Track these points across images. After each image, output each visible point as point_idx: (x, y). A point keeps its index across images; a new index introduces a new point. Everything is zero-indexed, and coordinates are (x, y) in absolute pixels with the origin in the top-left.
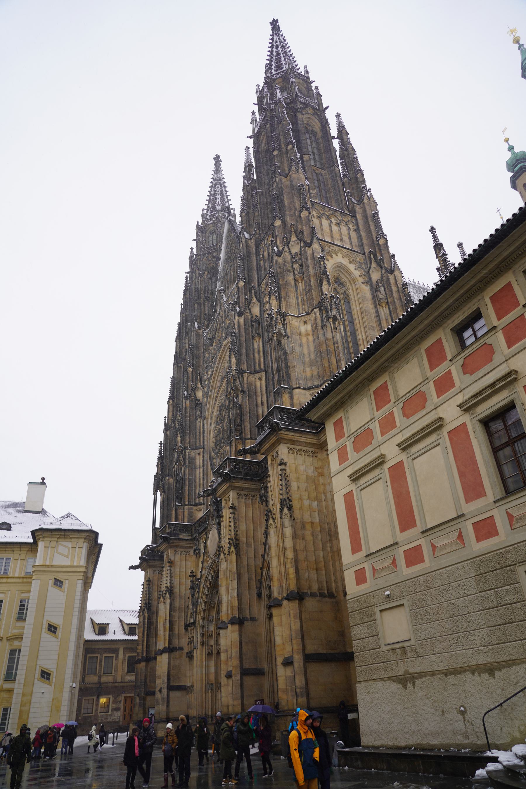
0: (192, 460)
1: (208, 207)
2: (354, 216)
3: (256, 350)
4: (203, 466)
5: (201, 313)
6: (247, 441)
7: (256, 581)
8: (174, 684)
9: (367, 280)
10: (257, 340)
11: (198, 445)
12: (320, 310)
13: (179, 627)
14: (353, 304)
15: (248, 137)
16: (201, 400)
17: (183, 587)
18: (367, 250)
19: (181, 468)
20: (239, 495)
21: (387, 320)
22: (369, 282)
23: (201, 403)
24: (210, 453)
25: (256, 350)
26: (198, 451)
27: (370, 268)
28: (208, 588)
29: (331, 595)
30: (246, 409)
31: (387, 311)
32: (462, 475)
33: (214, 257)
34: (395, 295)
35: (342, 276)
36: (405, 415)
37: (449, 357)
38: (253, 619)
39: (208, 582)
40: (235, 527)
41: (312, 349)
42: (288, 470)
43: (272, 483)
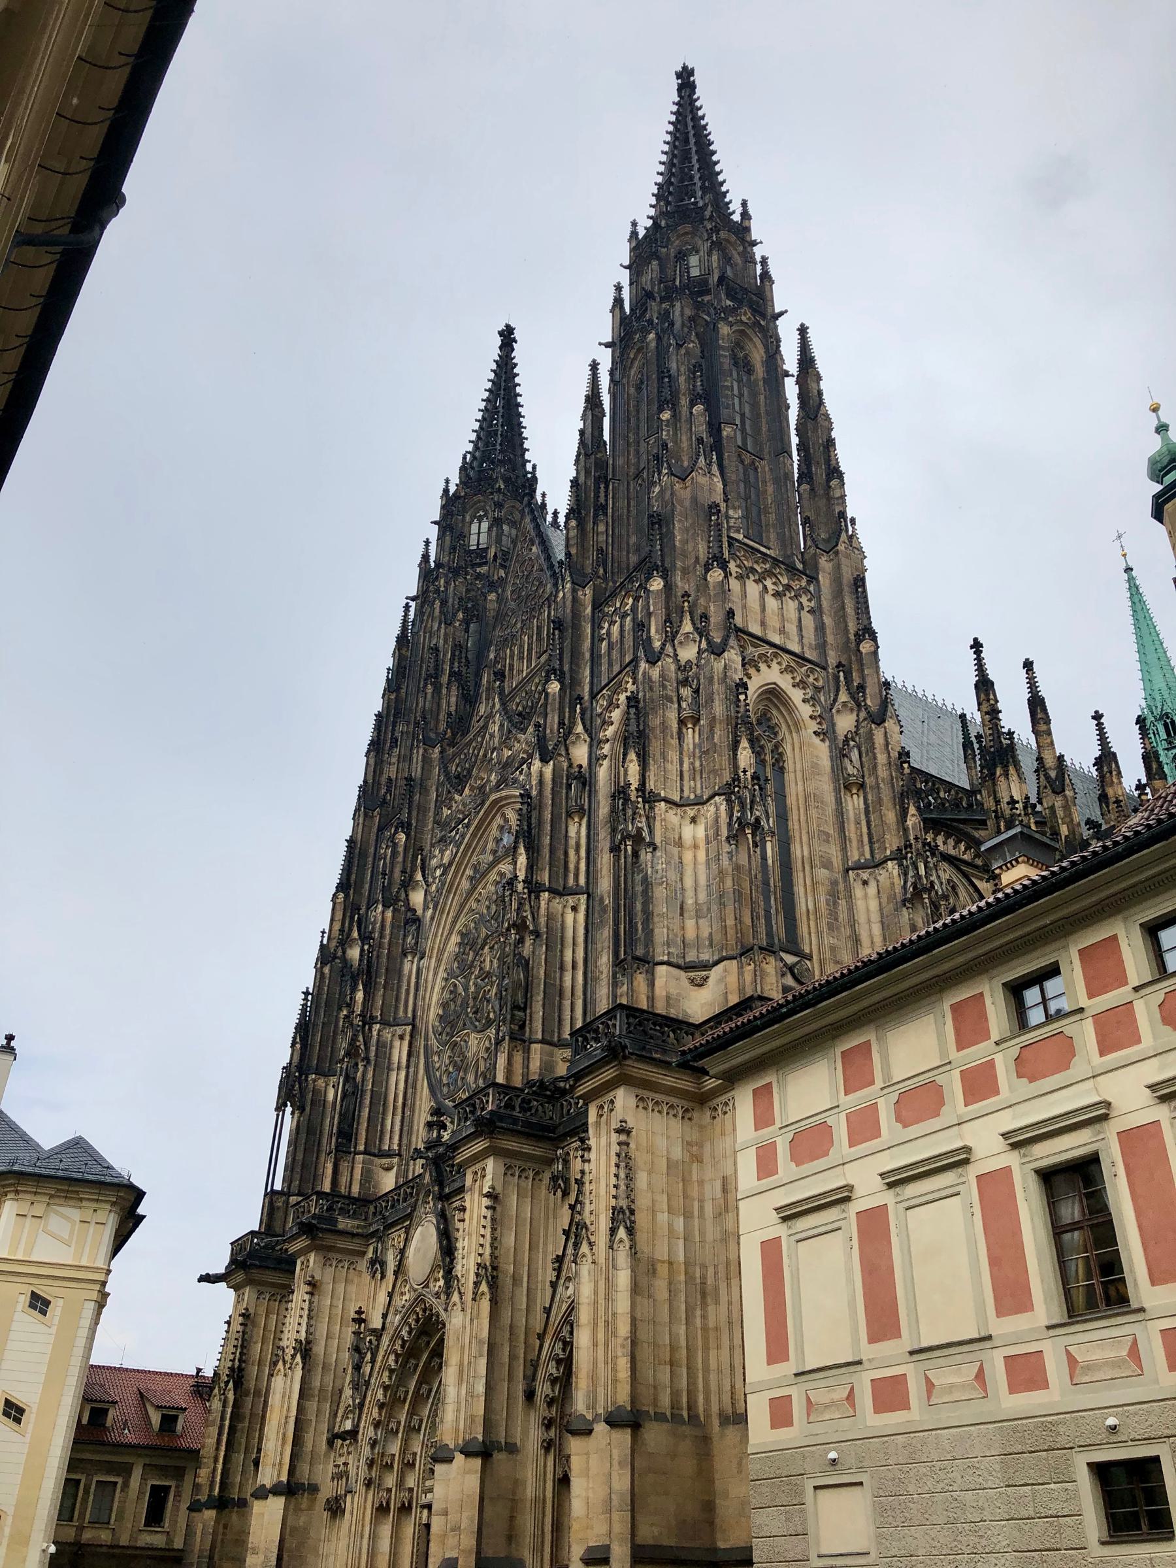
0: (384, 1049)
2: (813, 579)
3: (572, 842)
4: (408, 1067)
5: (439, 705)
6: (533, 1046)
7: (539, 1370)
9: (824, 726)
10: (576, 820)
11: (401, 1014)
12: (729, 802)
13: (316, 1438)
14: (789, 777)
16: (419, 912)
17: (335, 1347)
19: (357, 1064)
20: (509, 1168)
21: (858, 823)
22: (826, 733)
23: (418, 920)
24: (426, 1039)
26: (399, 1030)
27: (835, 701)
28: (397, 1356)
32: (994, 1262)
33: (479, 576)
34: (883, 772)
35: (774, 712)
36: (898, 1120)
37: (995, 1035)
38: (511, 1449)
40: (494, 1239)
41: (703, 880)
42: (632, 1146)
43: (593, 1165)
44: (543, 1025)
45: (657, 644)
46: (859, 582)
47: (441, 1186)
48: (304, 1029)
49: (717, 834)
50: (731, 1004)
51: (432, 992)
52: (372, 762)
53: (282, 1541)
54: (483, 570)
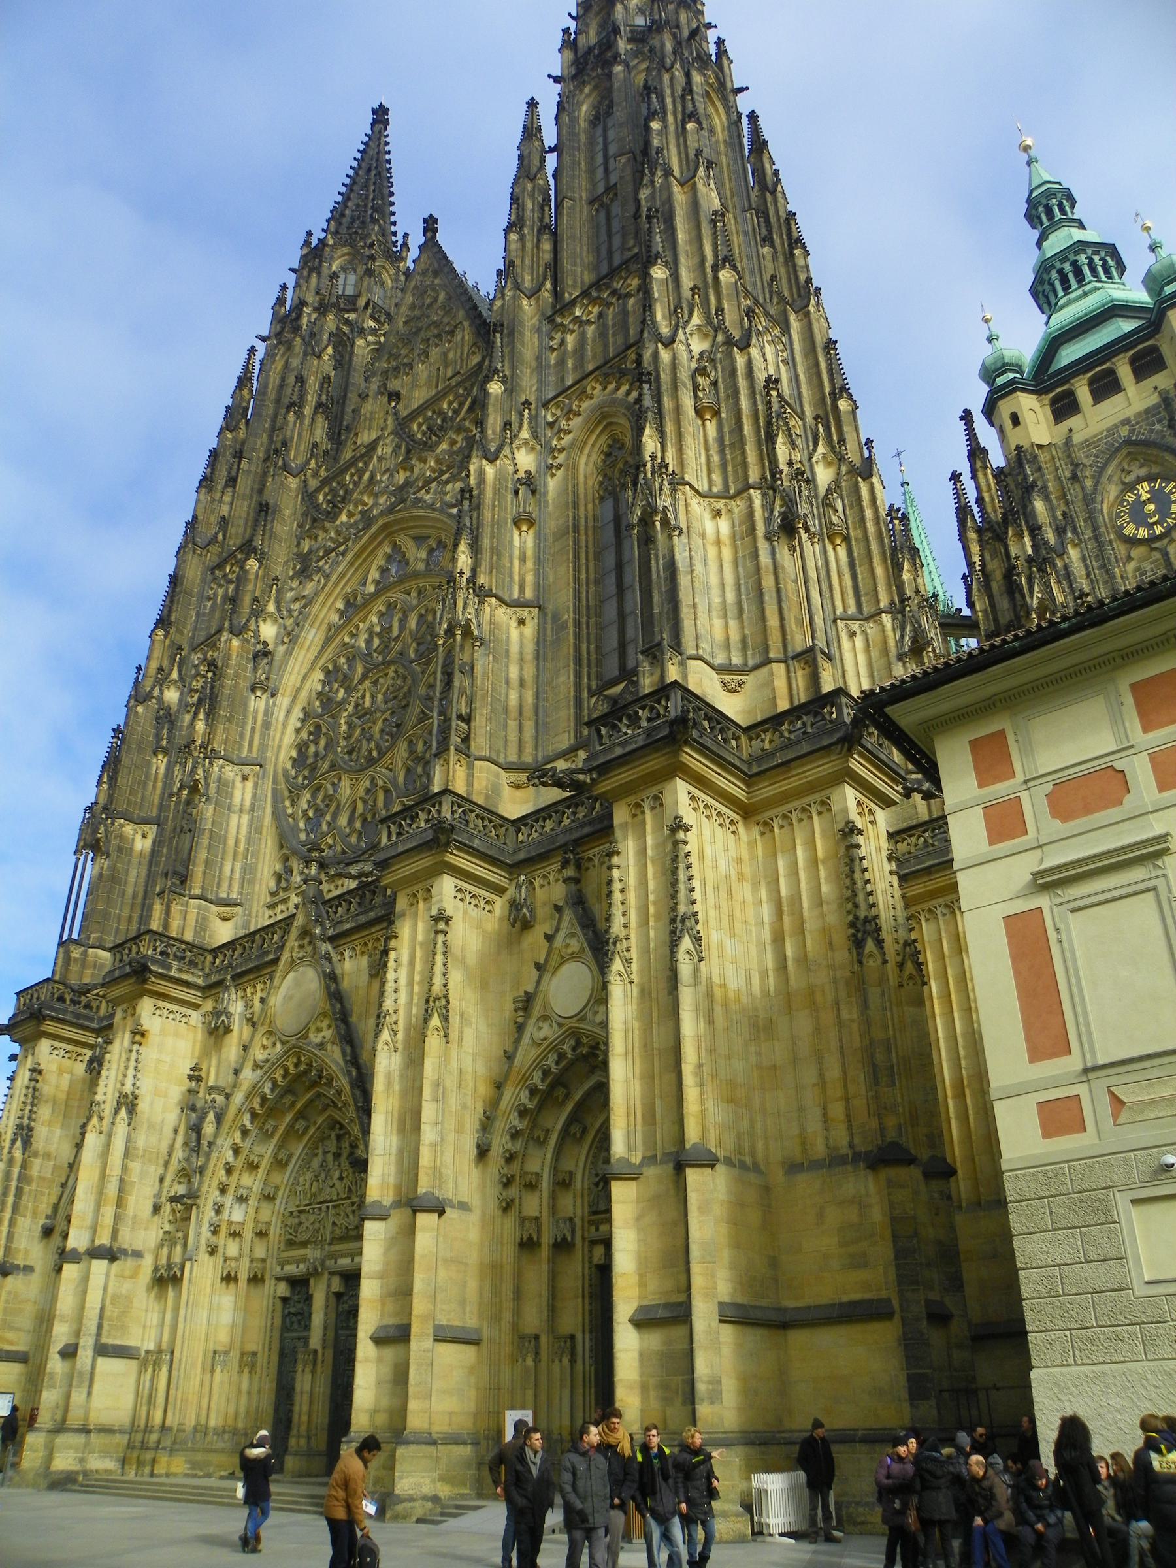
0: (224, 787)
3: (517, 552)
8: (110, 1341)
11: (245, 753)
12: (764, 495)
16: (271, 647)
18: (809, 413)
25: (517, 552)
26: (247, 770)
27: (815, 450)
29: (756, 1168)
31: (842, 552)
33: (347, 322)
39: (258, 1100)
42: (688, 848)
45: (665, 330)
46: (830, 345)
49: (752, 528)
50: (780, 710)
51: (283, 733)
52: (202, 497)
53: (102, 1309)
54: (352, 316)
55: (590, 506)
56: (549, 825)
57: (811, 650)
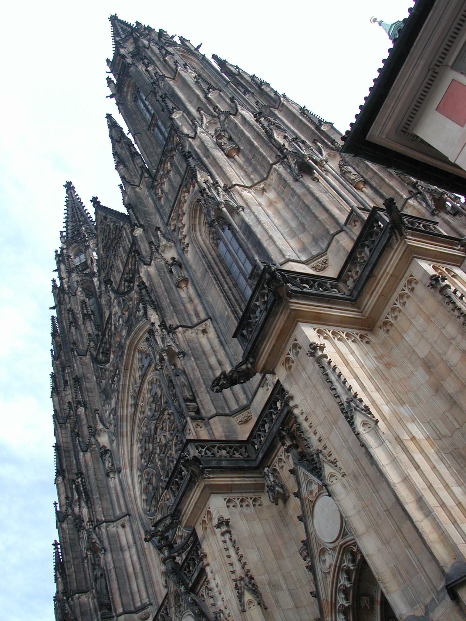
0: (114, 539)
1: (67, 229)
3: (186, 300)
4: (135, 542)
6: (211, 421)
10: (183, 285)
11: (118, 513)
12: (282, 163)
15: (107, 97)
20: (229, 501)
23: (108, 450)
24: (141, 519)
25: (186, 300)
30: (194, 375)
31: (367, 190)
33: (86, 275)
44: (213, 404)
46: (303, 111)
47: (185, 584)
48: (60, 568)
52: (56, 399)
54: (88, 271)
55: (213, 253)
56: (267, 426)
57: (352, 211)
